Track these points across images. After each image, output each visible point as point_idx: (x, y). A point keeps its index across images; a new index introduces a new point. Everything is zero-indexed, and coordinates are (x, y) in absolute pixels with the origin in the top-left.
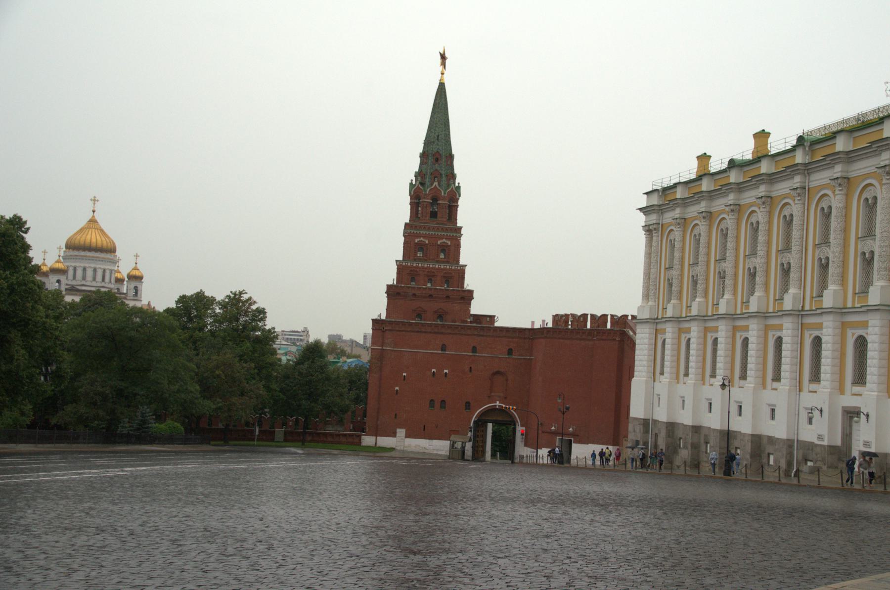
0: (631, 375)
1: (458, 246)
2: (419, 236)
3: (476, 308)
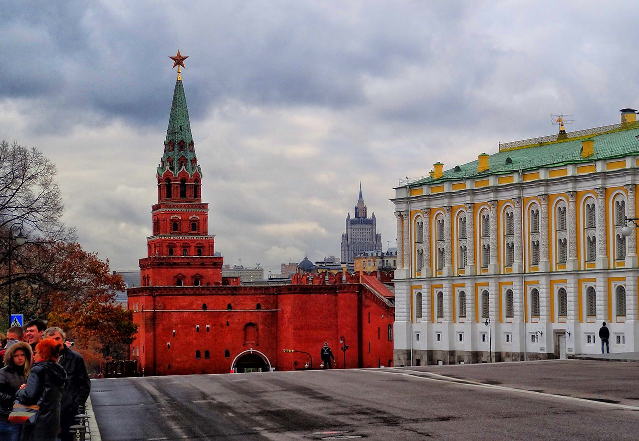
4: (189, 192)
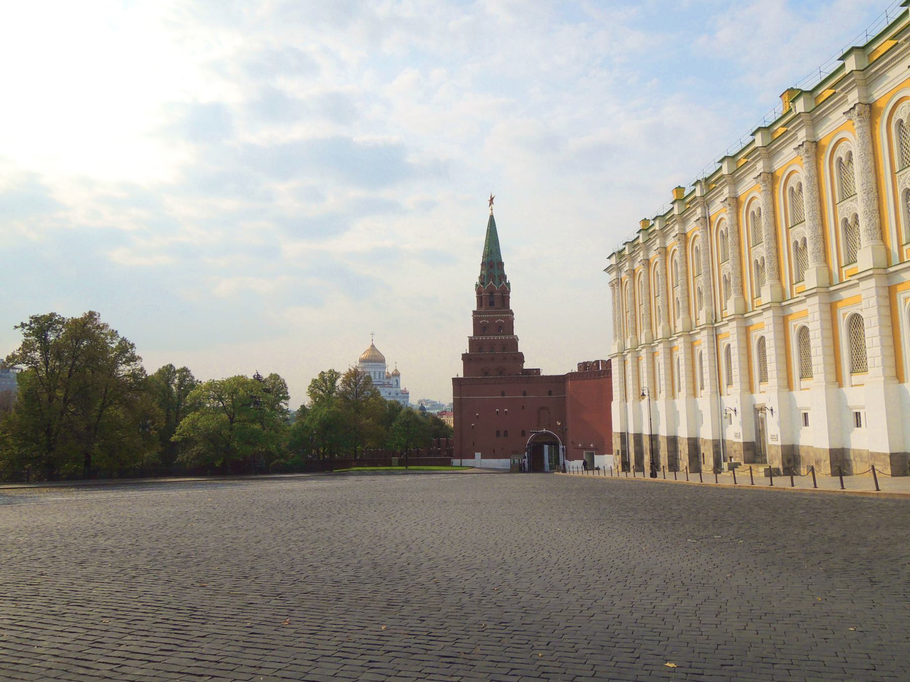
0: (610, 398)
2: (483, 319)
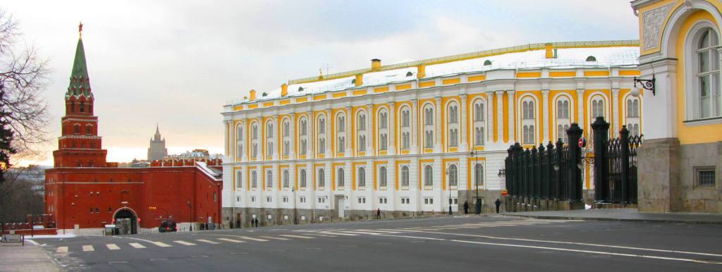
1: (96, 126)
3: (109, 159)
4: (87, 109)
